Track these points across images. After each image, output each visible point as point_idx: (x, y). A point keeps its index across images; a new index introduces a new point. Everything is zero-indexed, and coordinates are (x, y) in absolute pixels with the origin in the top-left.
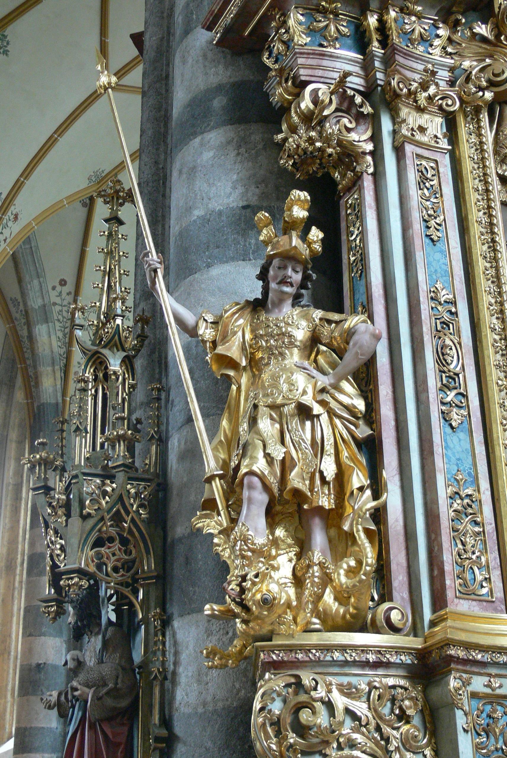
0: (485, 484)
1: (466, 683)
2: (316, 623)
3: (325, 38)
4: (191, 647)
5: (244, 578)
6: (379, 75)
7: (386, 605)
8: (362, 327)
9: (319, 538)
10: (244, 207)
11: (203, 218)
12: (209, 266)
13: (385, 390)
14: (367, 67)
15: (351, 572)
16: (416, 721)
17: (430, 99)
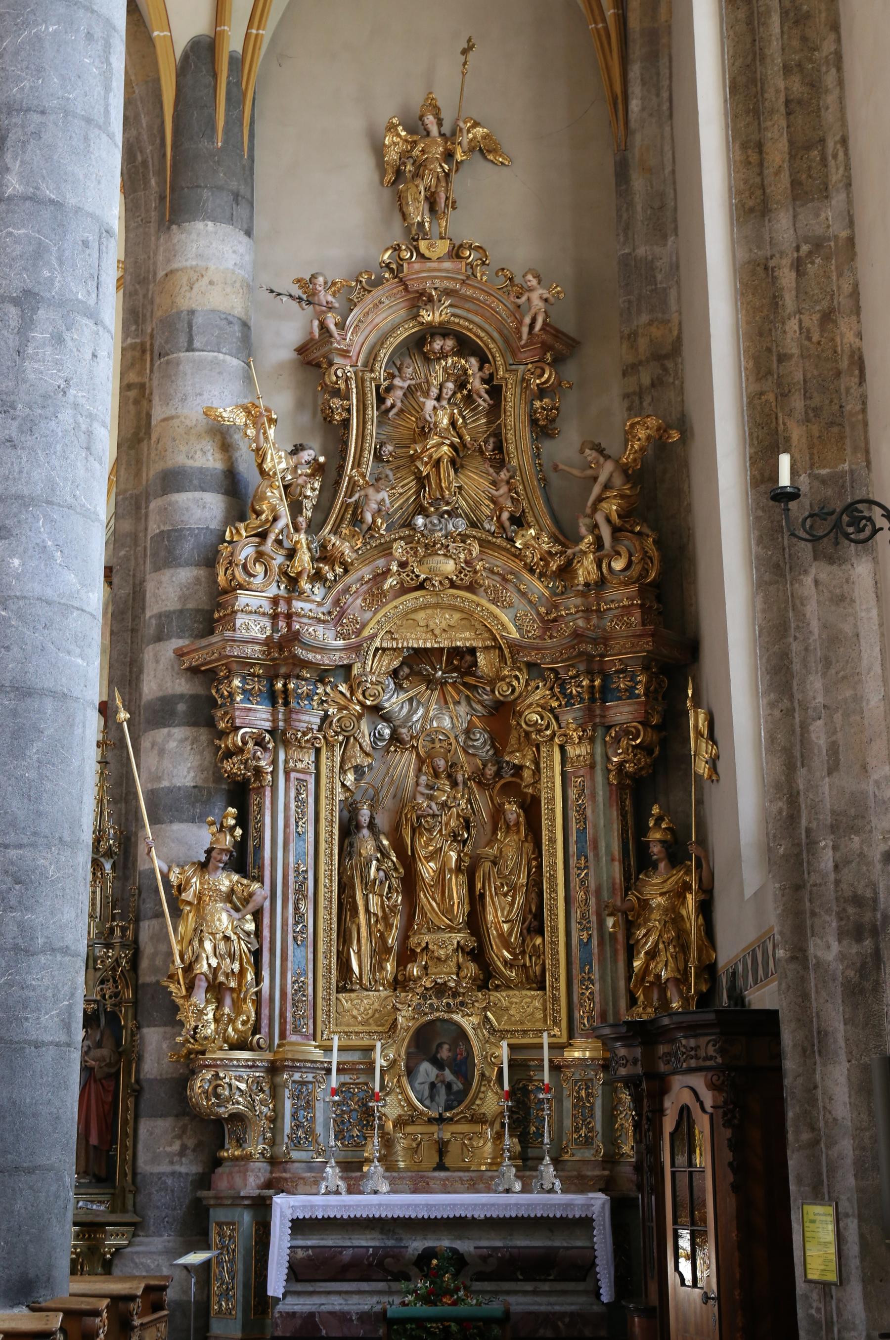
0: (310, 975)
1: (291, 1076)
2: (226, 1046)
3: (252, 695)
4: (154, 1044)
5: (196, 1027)
6: (281, 724)
7: (258, 1036)
8: (259, 892)
9: (228, 1001)
10: (194, 787)
11: (169, 788)
12: (171, 822)
13: (266, 921)
14: (274, 714)
15: (244, 1023)
16: (267, 1092)
17: (307, 741)
